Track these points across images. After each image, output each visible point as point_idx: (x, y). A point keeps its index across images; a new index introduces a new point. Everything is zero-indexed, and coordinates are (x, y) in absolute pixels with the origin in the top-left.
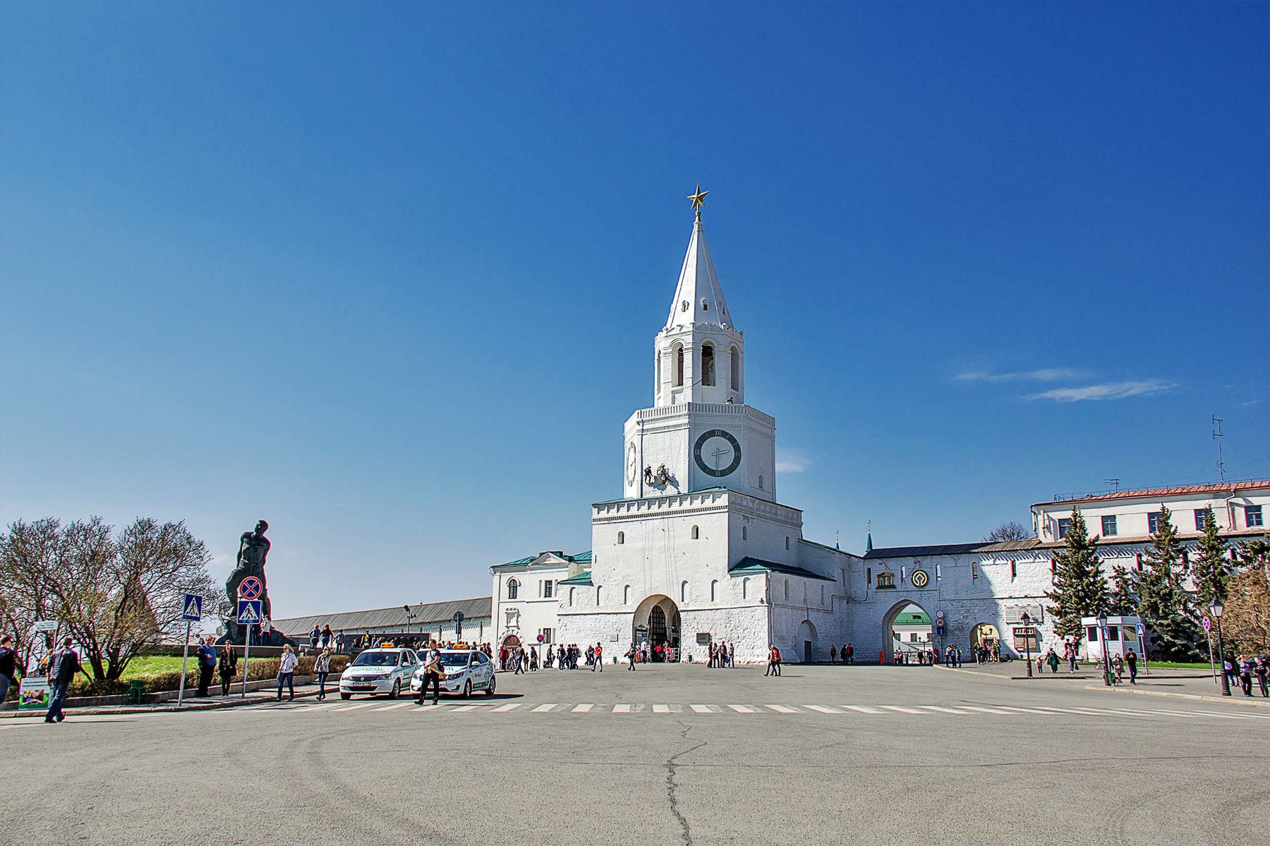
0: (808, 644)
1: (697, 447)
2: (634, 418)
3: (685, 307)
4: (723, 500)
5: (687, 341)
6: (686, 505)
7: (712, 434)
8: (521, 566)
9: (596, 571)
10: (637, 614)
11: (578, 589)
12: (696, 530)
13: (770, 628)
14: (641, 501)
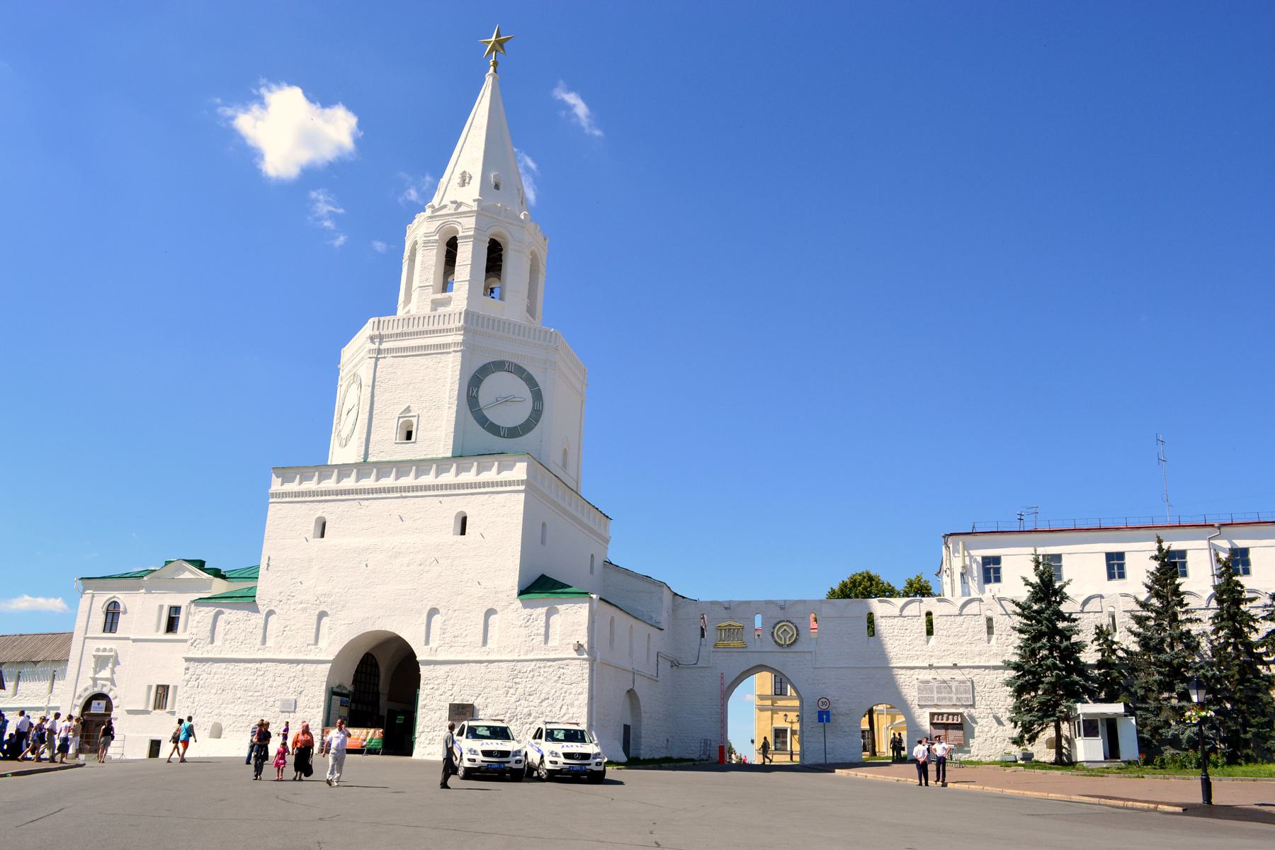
0: (627, 729)
1: (473, 383)
2: (368, 329)
3: (465, 180)
4: (520, 471)
5: (466, 227)
6: (449, 477)
7: (499, 366)
8: (132, 579)
9: (265, 589)
10: (336, 663)
11: (231, 615)
12: (464, 521)
13: (591, 698)
14: (363, 467)
